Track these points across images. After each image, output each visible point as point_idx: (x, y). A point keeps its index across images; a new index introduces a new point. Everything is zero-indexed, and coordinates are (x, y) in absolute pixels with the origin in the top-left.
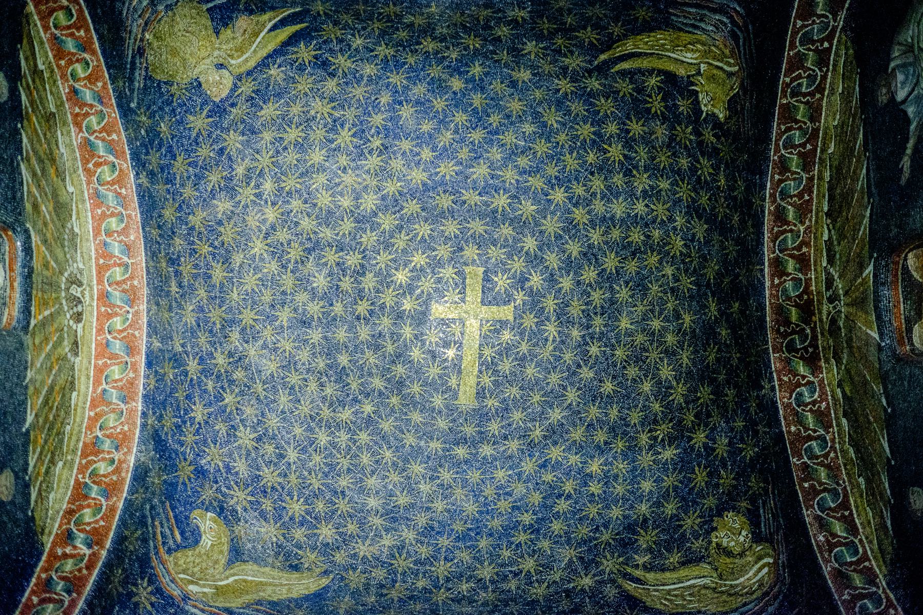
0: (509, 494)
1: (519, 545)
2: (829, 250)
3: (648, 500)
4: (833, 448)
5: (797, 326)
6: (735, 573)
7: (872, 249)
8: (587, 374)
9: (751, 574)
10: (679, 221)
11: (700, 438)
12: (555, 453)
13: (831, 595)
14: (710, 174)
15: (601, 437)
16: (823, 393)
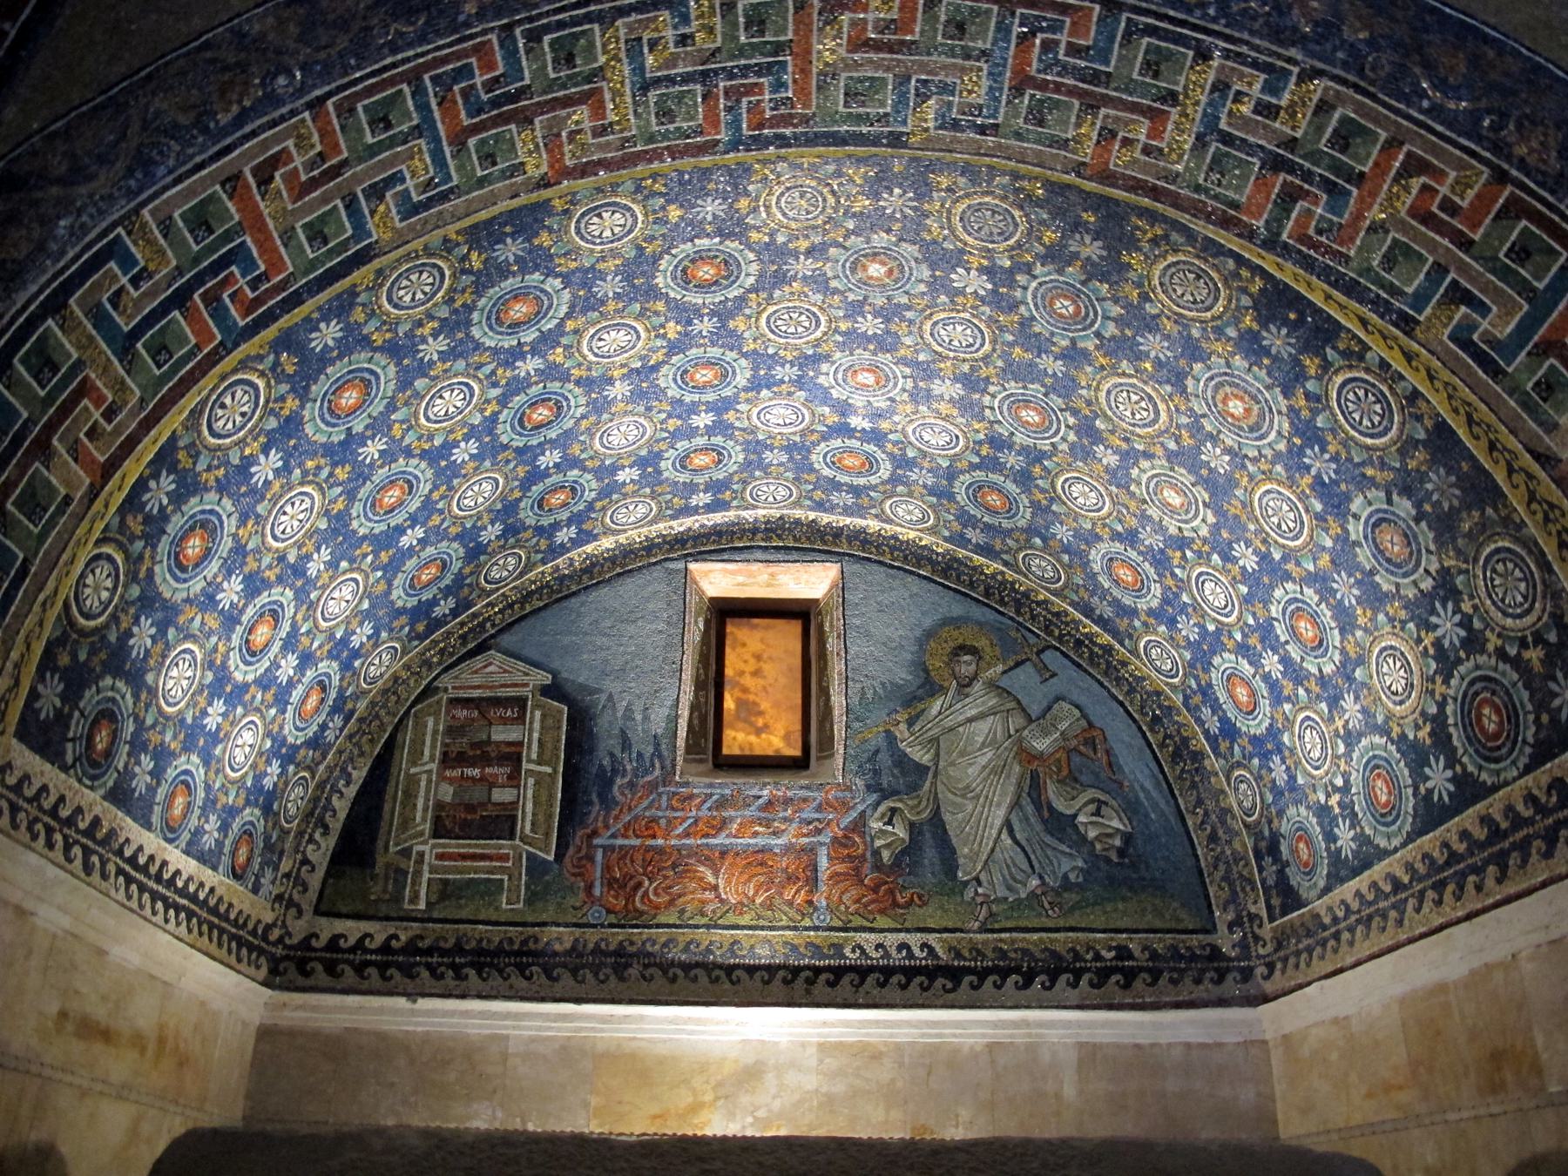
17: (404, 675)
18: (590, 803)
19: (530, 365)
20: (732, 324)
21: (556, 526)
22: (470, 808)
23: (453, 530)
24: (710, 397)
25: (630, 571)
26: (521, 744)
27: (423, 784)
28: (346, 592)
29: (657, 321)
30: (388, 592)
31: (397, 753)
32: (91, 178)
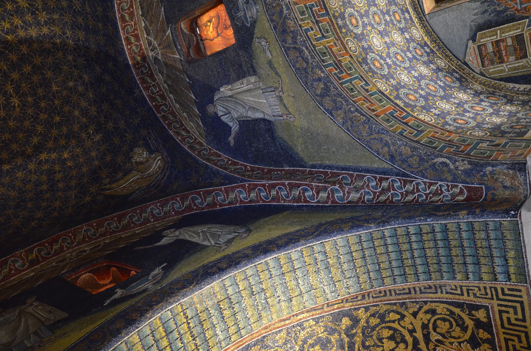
0: (30, 181)
1: (48, 199)
2: (146, 30)
3: (97, 159)
4: (170, 107)
5: (142, 64)
6: (147, 169)
7: (168, 24)
8: (43, 116)
9: (154, 166)
10: (69, 33)
11: (110, 125)
12: (43, 156)
13: (191, 155)
14: (80, 7)
15: (63, 142)
16: (159, 88)
17: (478, 82)
18: (507, 15)
19: (388, 60)
20: (363, 13)
21: (426, 52)
22: (516, 50)
23: (435, 75)
24: (382, 17)
25: (432, 30)
26: (492, 42)
27: (511, 66)
28: (461, 95)
29: (368, 32)
30: (457, 87)
31: (504, 77)
32: (386, 141)
